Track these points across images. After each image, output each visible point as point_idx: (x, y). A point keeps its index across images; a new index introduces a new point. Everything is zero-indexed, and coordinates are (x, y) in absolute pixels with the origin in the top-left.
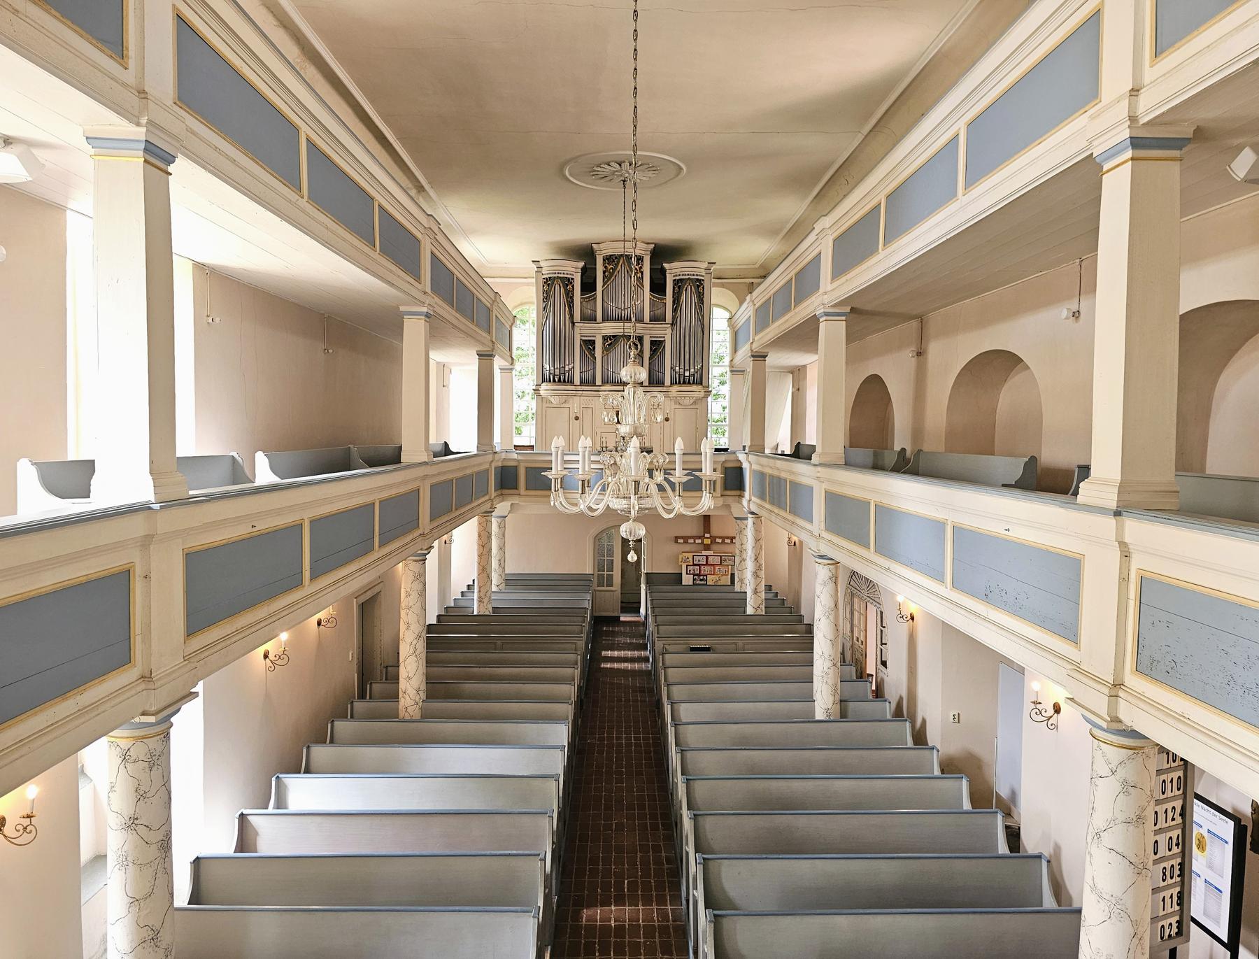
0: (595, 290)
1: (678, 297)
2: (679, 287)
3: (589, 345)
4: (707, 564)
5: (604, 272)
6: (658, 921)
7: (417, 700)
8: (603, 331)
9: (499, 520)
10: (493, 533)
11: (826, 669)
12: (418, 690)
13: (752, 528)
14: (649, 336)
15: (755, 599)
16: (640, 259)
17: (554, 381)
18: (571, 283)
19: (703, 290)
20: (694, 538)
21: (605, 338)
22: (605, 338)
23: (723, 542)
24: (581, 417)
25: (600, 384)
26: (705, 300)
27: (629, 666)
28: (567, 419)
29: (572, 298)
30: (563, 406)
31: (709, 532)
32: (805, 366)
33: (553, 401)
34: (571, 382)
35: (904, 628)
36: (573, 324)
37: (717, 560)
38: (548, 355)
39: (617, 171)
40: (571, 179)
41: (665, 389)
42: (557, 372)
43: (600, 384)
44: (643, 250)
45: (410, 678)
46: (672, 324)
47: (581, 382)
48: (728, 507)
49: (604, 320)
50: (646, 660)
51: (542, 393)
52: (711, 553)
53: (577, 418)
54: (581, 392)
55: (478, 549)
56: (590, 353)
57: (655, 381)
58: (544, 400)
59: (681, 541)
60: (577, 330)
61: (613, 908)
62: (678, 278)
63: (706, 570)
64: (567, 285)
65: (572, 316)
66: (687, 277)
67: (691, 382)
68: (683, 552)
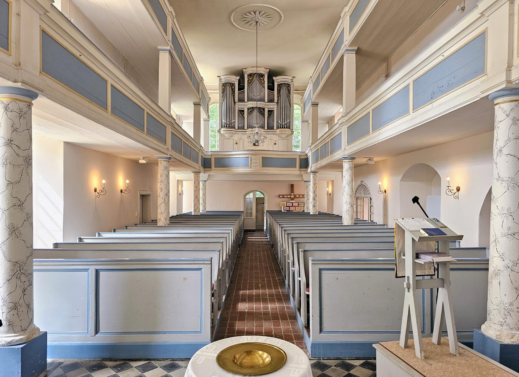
0: (244, 88)
1: (279, 91)
2: (280, 87)
3: (242, 112)
4: (292, 206)
5: (248, 81)
6: (275, 293)
7: (166, 223)
8: (248, 106)
9: (203, 182)
10: (200, 188)
11: (348, 208)
12: (166, 219)
13: (313, 179)
15: (314, 210)
16: (263, 75)
17: (227, 127)
18: (234, 85)
19: (290, 89)
20: (287, 195)
21: (248, 109)
22: (248, 109)
23: (299, 197)
24: (238, 143)
25: (247, 129)
26: (291, 93)
27: (260, 240)
28: (232, 144)
29: (234, 92)
30: (230, 138)
31: (293, 193)
32: (334, 116)
33: (226, 136)
34: (234, 128)
35: (382, 196)
36: (235, 103)
37: (297, 205)
38: (224, 117)
39: (254, 18)
40: (234, 23)
41: (274, 131)
42: (228, 123)
43: (247, 129)
44: (263, 71)
45: (162, 213)
46: (277, 103)
47: (238, 128)
48: (301, 176)
49: (248, 100)
50: (268, 239)
51: (222, 132)
52: (294, 201)
53: (236, 143)
54: (238, 132)
55: (194, 189)
56: (242, 116)
57: (270, 127)
58: (223, 136)
59: (281, 196)
60: (236, 106)
61: (254, 290)
63: (292, 209)
64: (232, 86)
65: (234, 100)
66: (283, 83)
67: (285, 127)
68: (282, 201)
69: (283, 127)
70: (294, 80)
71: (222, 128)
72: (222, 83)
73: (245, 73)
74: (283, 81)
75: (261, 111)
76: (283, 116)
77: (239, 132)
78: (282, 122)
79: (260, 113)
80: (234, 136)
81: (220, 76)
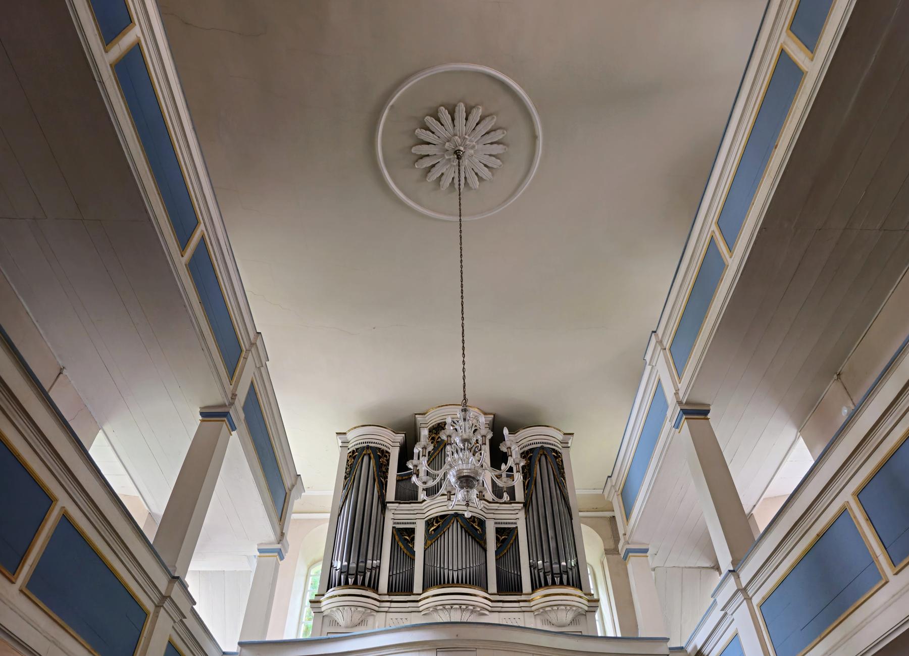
2: (530, 458)
3: (404, 535)
14: (492, 522)
17: (347, 583)
18: (386, 456)
21: (429, 523)
34: (375, 587)
41: (523, 598)
42: (353, 565)
51: (326, 604)
54: (388, 604)
56: (407, 547)
58: (327, 620)
60: (389, 515)
62: (526, 449)
64: (380, 457)
66: (539, 445)
69: (557, 580)
70: (570, 442)
71: (328, 589)
72: (349, 451)
73: (423, 425)
74: (538, 441)
75: (472, 526)
76: (553, 544)
77: (393, 605)
78: (548, 564)
79: (469, 535)
80: (370, 620)
81: (345, 434)
